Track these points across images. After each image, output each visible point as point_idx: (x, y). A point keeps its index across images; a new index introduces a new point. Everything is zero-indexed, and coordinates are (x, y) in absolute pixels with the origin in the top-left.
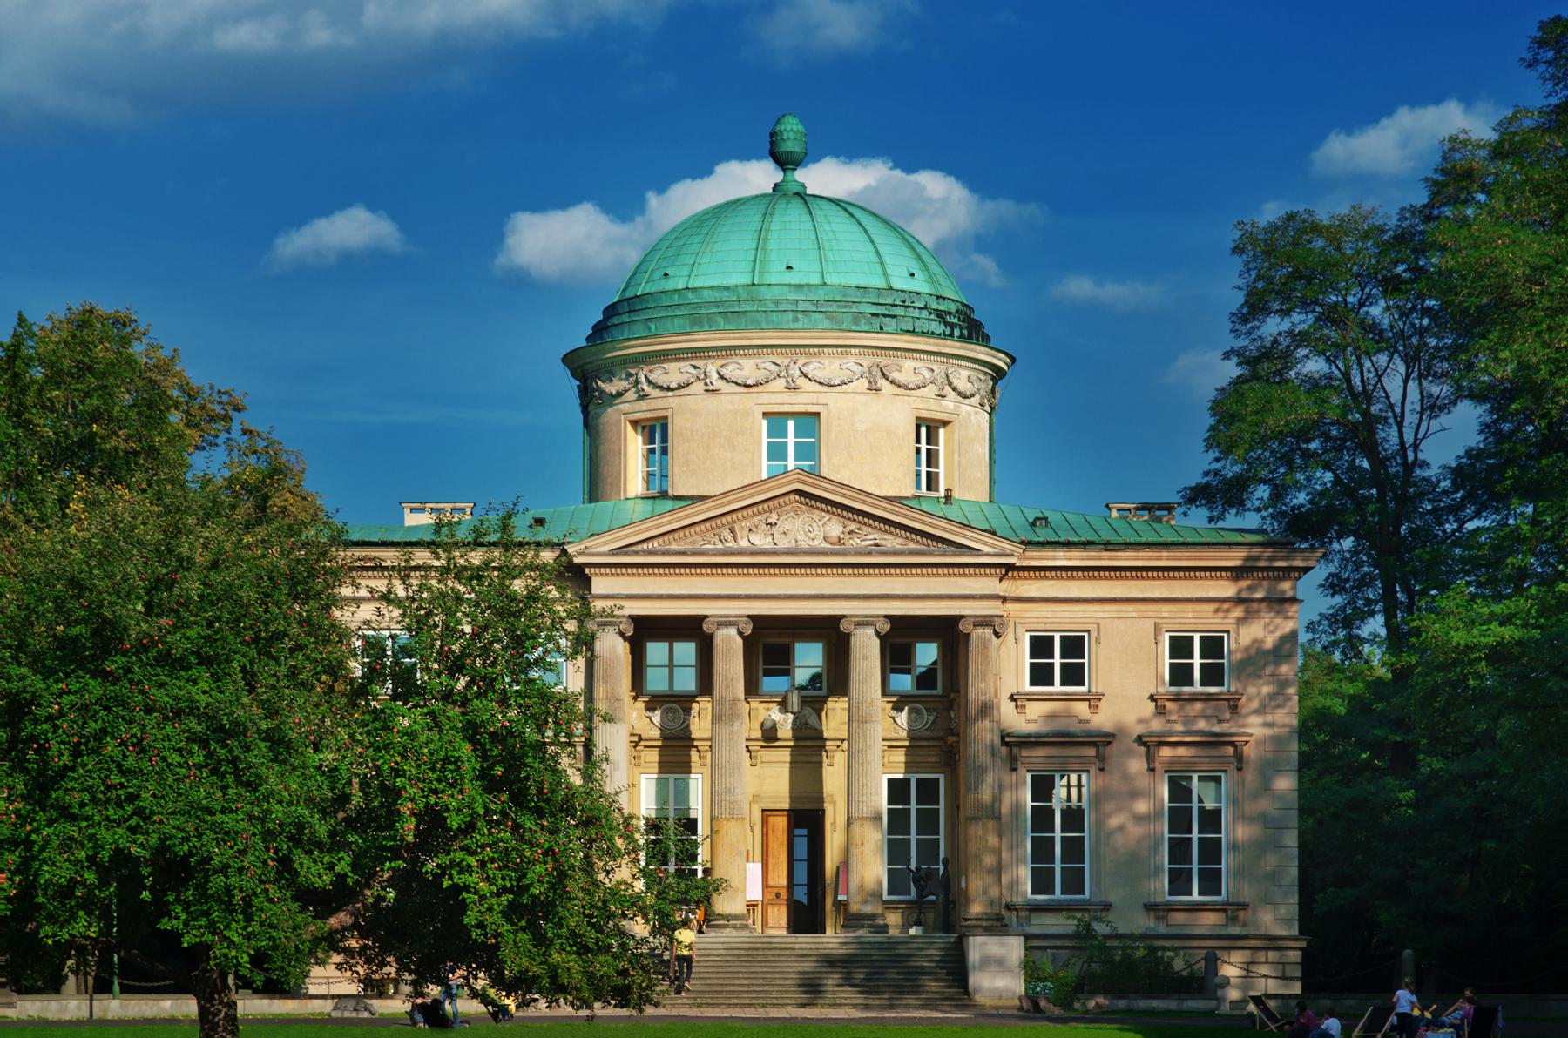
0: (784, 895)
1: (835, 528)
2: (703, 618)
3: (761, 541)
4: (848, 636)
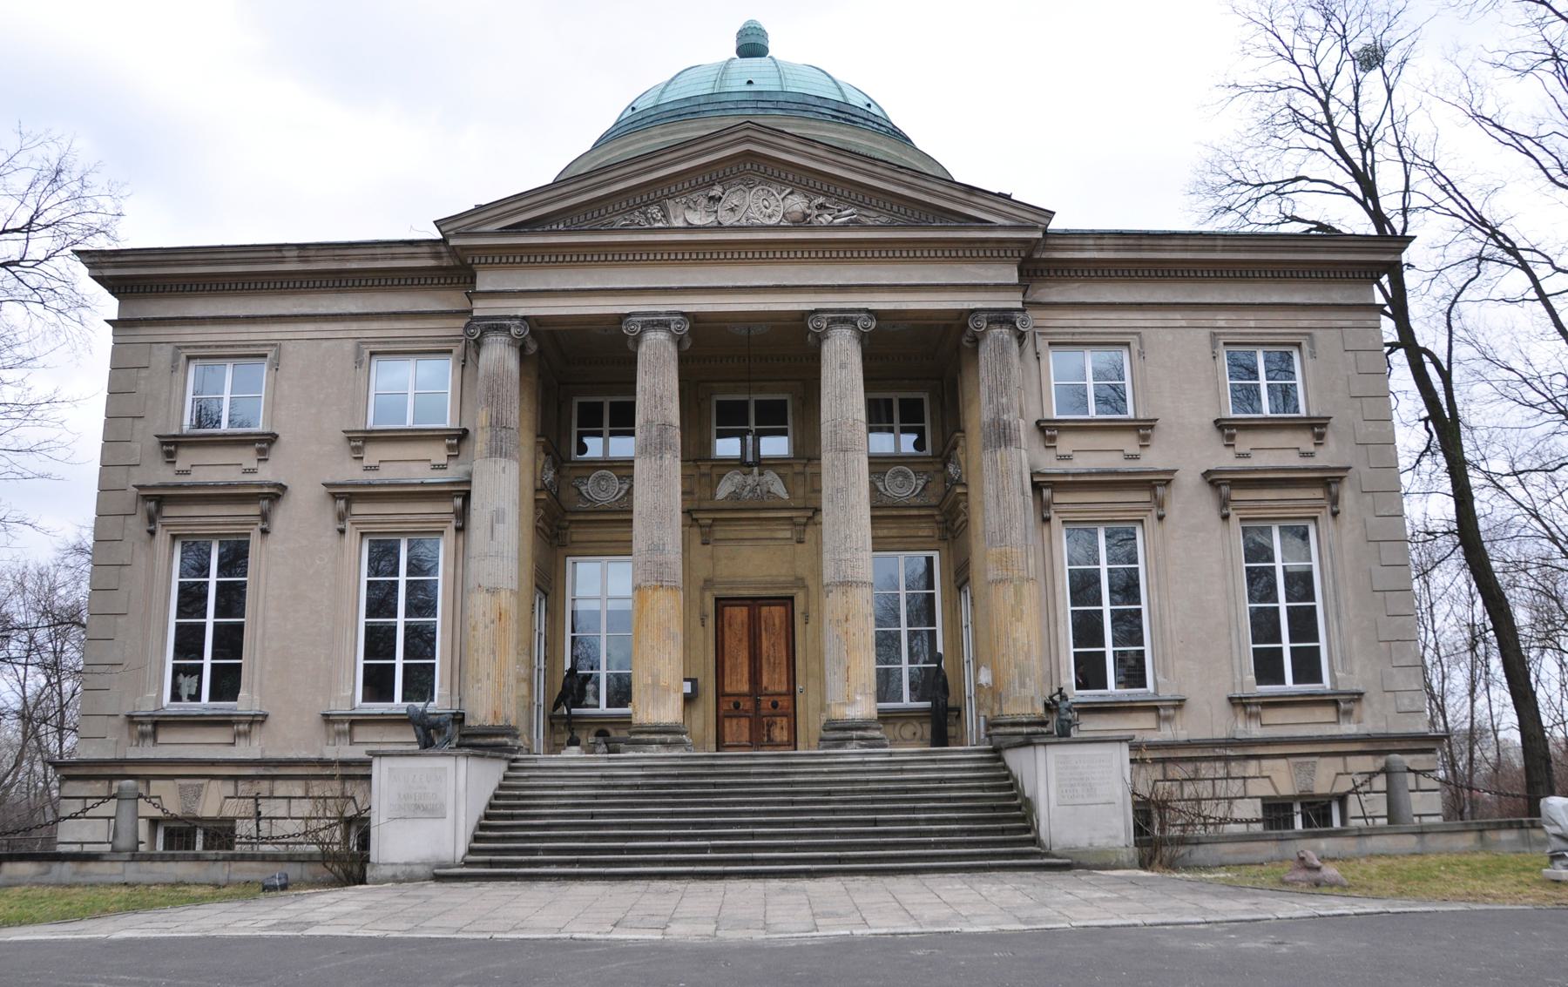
0: (746, 704)
1: (797, 203)
2: (621, 318)
3: (696, 219)
4: (820, 338)
